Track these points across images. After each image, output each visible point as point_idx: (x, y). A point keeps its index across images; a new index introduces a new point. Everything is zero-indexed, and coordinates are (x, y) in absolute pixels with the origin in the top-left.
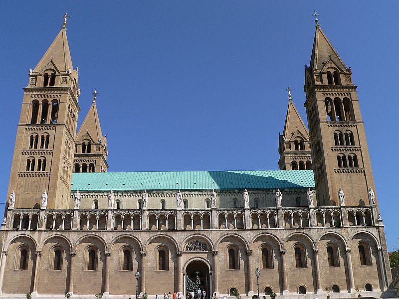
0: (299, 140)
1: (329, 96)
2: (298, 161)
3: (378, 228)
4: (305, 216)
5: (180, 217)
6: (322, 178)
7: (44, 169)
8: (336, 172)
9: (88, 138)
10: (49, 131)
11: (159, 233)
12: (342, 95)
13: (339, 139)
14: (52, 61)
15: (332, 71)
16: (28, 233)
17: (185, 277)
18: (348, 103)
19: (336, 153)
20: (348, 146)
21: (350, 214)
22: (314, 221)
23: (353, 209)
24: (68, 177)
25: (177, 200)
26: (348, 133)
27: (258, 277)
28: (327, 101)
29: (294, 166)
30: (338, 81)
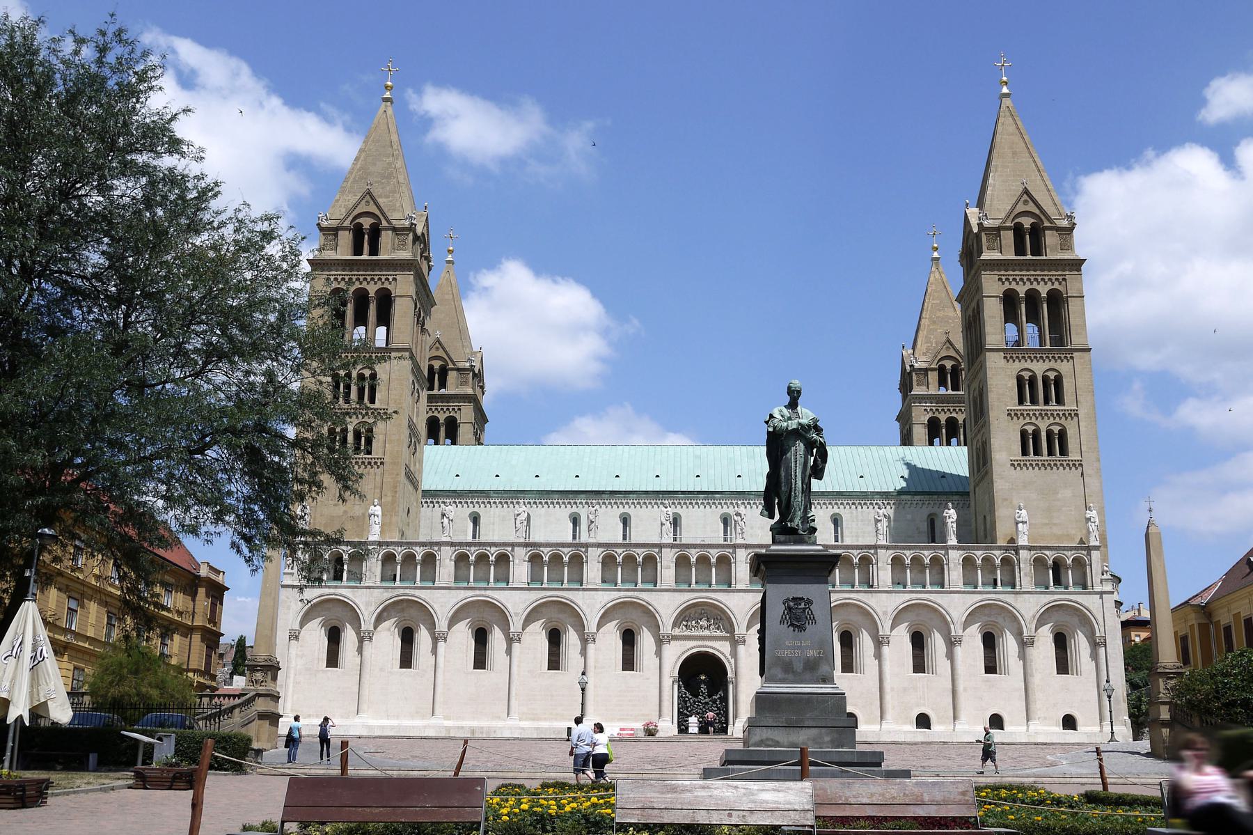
2: (943, 418)
3: (1101, 593)
4: (938, 564)
5: (668, 559)
9: (441, 353)
13: (1026, 388)
17: (676, 686)
19: (1016, 426)
21: (1039, 563)
22: (955, 574)
24: (417, 464)
25: (662, 524)
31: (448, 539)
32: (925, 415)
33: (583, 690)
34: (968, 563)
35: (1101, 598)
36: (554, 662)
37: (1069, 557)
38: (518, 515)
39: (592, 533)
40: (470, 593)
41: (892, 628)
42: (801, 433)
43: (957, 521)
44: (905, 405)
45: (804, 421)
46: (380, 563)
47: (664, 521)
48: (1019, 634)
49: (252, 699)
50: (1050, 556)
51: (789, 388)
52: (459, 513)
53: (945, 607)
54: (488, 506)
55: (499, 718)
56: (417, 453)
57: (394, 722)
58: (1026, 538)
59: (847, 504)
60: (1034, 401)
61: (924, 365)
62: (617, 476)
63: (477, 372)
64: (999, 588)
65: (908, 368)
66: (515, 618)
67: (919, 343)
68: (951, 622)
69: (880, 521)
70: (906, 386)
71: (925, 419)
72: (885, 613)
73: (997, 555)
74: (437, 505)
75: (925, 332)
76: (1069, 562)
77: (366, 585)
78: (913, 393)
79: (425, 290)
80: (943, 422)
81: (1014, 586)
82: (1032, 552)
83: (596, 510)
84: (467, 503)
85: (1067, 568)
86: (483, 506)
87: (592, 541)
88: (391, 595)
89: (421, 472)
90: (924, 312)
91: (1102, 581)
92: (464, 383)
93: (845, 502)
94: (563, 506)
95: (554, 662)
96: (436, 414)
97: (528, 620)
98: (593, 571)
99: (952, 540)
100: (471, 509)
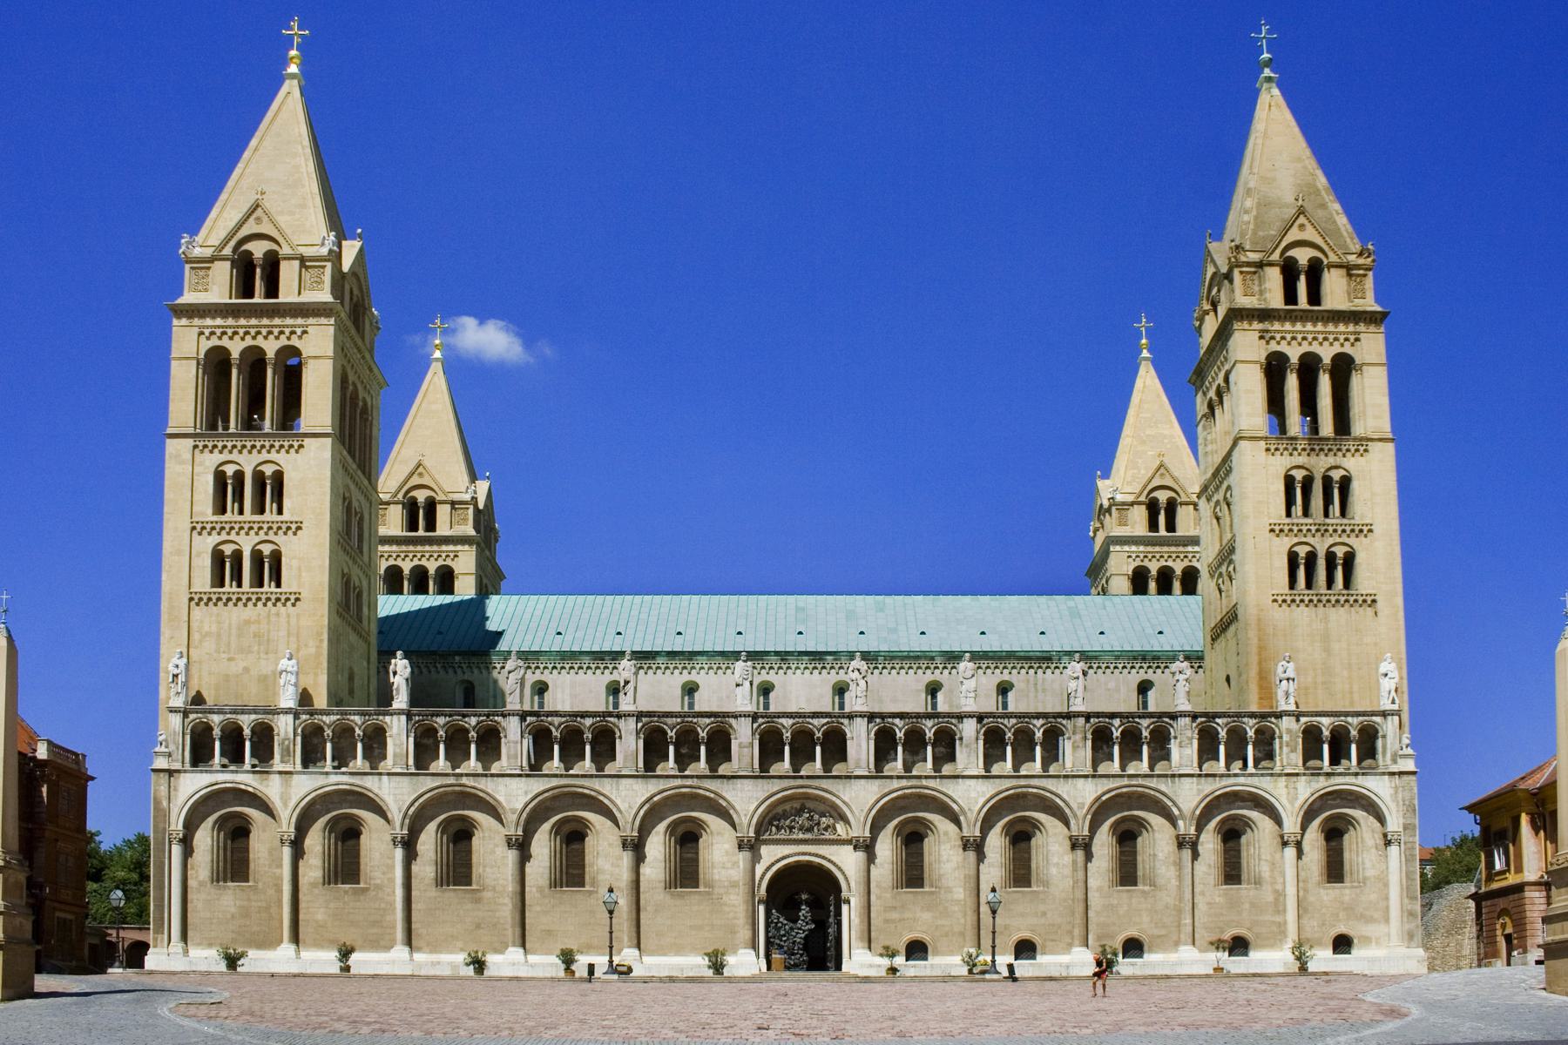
0: (1162, 496)
5: (744, 737)
11: (679, 782)
29: (1139, 582)
61: (1130, 498)
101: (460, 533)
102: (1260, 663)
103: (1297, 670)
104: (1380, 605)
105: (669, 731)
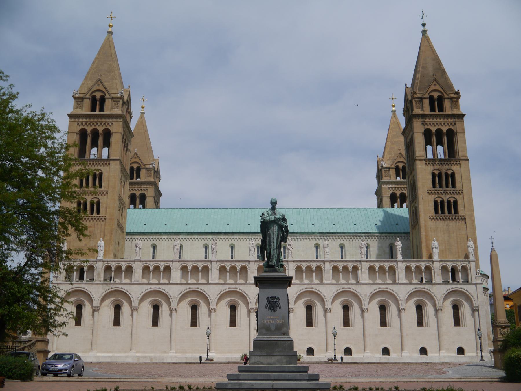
1: (429, 127)
2: (398, 193)
3: (476, 284)
4: (392, 269)
6: (416, 225)
7: (98, 213)
8: (432, 220)
10: (102, 168)
12: (446, 126)
14: (99, 80)
15: (436, 95)
16: (84, 286)
18: (451, 135)
19: (432, 198)
20: (447, 189)
21: (444, 269)
22: (401, 275)
23: (449, 263)
24: (123, 219)
25: (250, 250)
26: (450, 172)
27: (335, 337)
28: (428, 134)
30: (441, 109)
31: (138, 258)
32: (389, 192)
33: (208, 337)
34: (408, 269)
35: (476, 286)
36: (194, 323)
37: (459, 265)
38: (175, 246)
39: (214, 255)
40: (149, 286)
41: (370, 302)
42: (275, 222)
43: (402, 248)
44: (379, 186)
45: (277, 216)
46: (103, 271)
47: (251, 248)
48: (435, 305)
49: (35, 343)
50: (450, 265)
51: (271, 201)
52: (145, 244)
53: (396, 292)
54: (161, 240)
55: (165, 352)
56: (124, 214)
57: (110, 355)
58: (437, 256)
59: (348, 238)
60: (441, 186)
61: (388, 166)
62: (228, 225)
63: (156, 170)
64: (424, 282)
65: (380, 167)
66: (173, 300)
67: (386, 155)
68: (399, 300)
69: (362, 248)
70: (379, 177)
71: (389, 194)
72: (366, 295)
73: (423, 265)
74: (134, 240)
75: (389, 149)
76: (459, 268)
77: (96, 282)
78: (382, 180)
79: (128, 129)
80: (398, 195)
81: (432, 282)
82: (441, 263)
83: (216, 243)
84: (149, 239)
85: (458, 271)
86: (158, 240)
87: (214, 259)
88: (109, 288)
89: (125, 223)
90: (388, 139)
91: (476, 278)
92: (149, 176)
93: (346, 238)
94: (200, 240)
95: (194, 323)
96: (135, 192)
97: (181, 299)
98: (214, 274)
99: (400, 257)
100: (152, 242)
101: (148, 181)
102: (426, 241)
103: (438, 244)
104: (467, 219)
105: (227, 267)
